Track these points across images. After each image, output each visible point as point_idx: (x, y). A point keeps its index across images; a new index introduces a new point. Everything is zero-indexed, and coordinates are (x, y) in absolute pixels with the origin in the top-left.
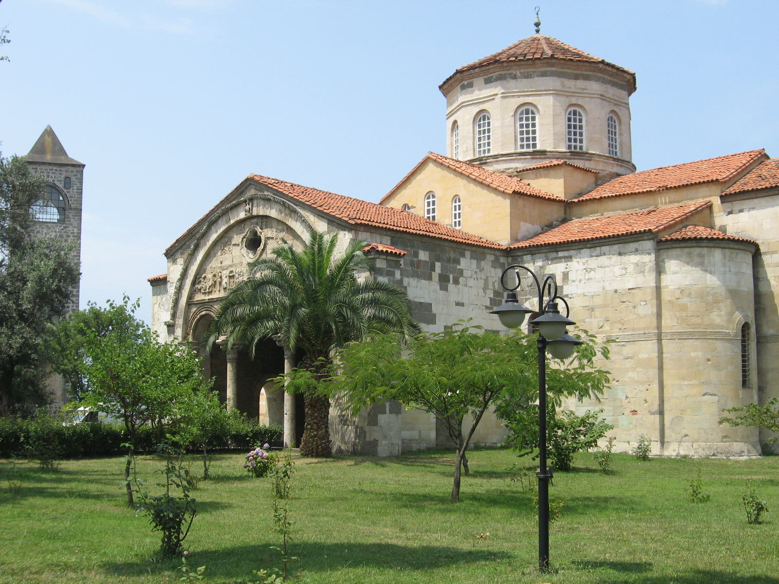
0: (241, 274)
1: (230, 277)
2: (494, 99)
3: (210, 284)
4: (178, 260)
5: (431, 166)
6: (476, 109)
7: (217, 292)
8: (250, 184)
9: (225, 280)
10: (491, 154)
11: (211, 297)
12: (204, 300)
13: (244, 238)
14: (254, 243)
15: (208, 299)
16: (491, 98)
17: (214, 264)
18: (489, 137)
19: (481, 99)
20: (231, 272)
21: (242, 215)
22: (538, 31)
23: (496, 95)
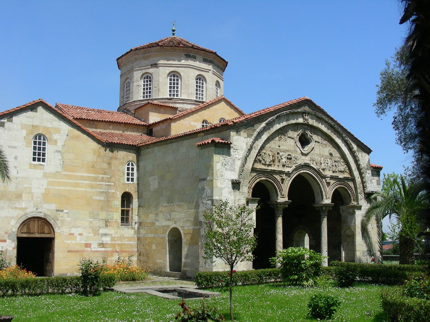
0: (297, 159)
1: (288, 158)
2: (208, 72)
3: (272, 160)
4: (242, 133)
5: (223, 103)
6: (198, 73)
7: (276, 166)
8: (306, 103)
9: (284, 160)
10: (179, 97)
11: (270, 168)
12: (267, 169)
13: (298, 135)
14: (304, 141)
15: (271, 170)
16: (207, 71)
17: (273, 144)
18: (202, 91)
19: (201, 68)
20: (289, 155)
21: (301, 120)
22: (174, 34)
23: (210, 70)
